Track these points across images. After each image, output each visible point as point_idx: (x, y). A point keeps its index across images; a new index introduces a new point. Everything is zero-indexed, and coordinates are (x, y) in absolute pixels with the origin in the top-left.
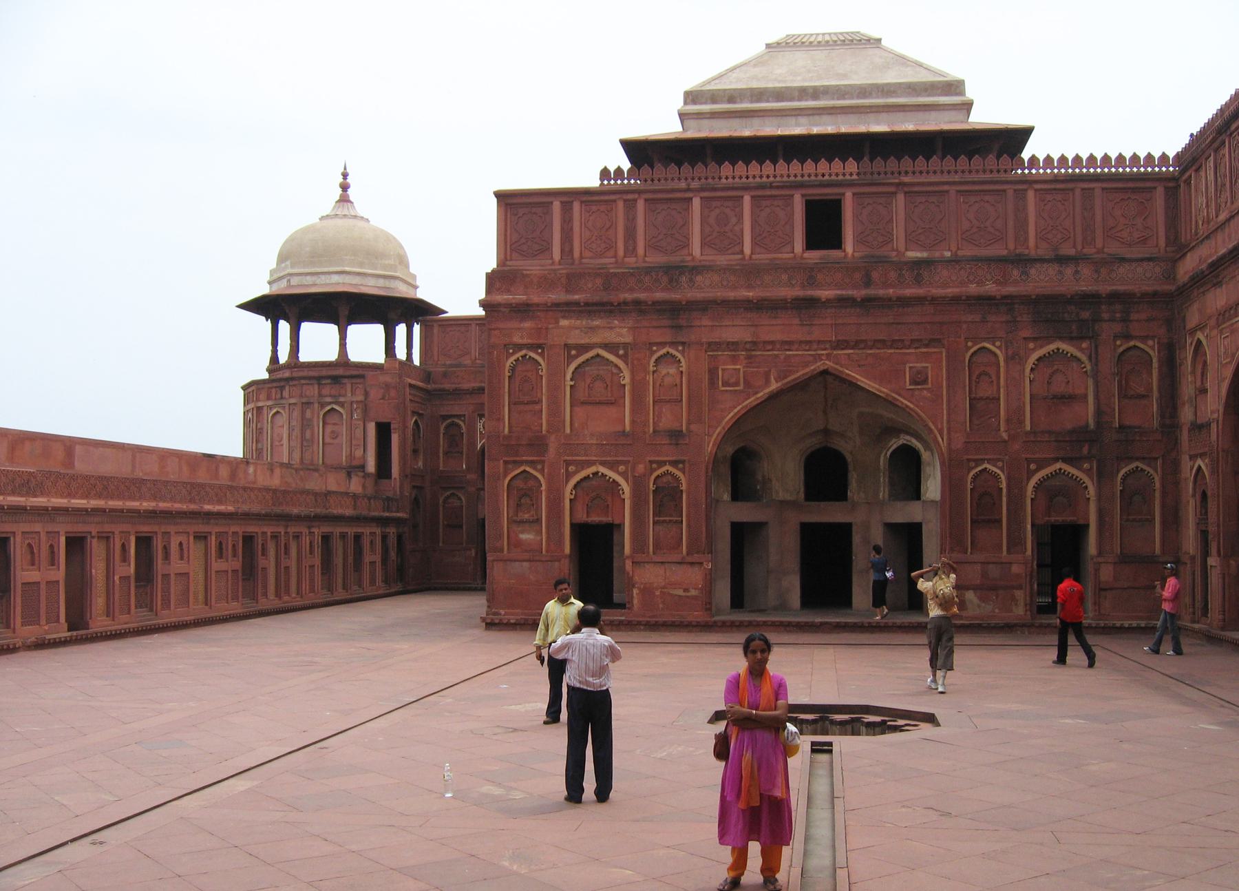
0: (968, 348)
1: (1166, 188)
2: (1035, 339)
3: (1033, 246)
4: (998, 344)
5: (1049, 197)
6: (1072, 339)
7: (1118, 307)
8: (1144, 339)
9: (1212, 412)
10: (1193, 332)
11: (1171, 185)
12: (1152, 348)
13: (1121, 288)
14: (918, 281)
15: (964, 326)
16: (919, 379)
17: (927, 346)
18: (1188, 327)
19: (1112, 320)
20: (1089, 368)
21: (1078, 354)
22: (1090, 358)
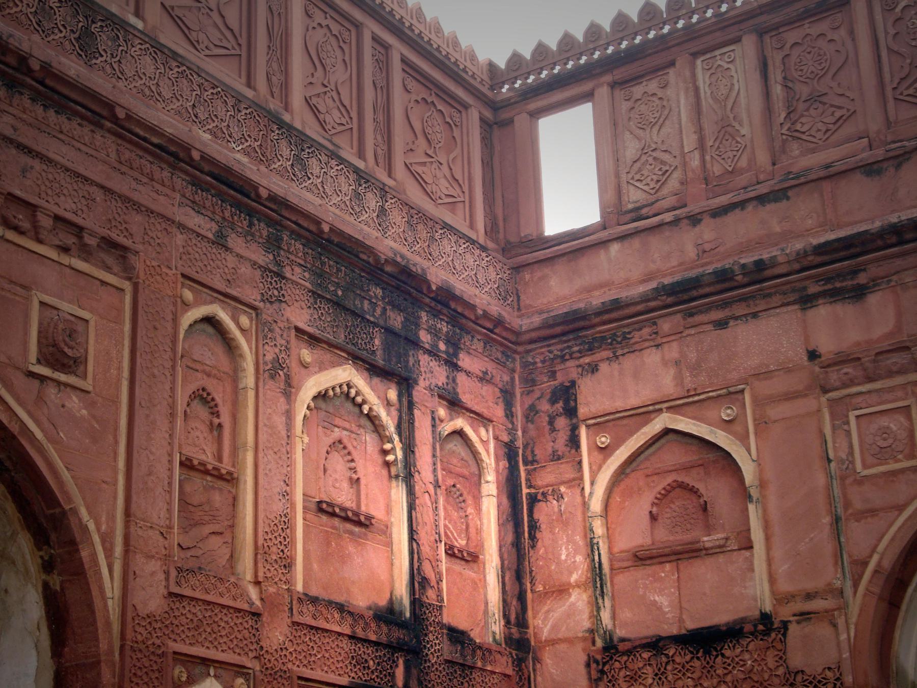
0: (186, 306)
1: (482, 120)
2: (313, 340)
3: (299, 117)
4: (245, 321)
5: (319, 17)
6: (374, 370)
7: (444, 327)
8: (480, 419)
9: (781, 599)
10: (643, 414)
11: (488, 114)
12: (485, 443)
13: (460, 286)
14: (85, 46)
15: (180, 238)
16: (61, 354)
17: (85, 252)
18: (582, 411)
19: (433, 353)
20: (400, 454)
21: (383, 413)
22: (399, 427)
